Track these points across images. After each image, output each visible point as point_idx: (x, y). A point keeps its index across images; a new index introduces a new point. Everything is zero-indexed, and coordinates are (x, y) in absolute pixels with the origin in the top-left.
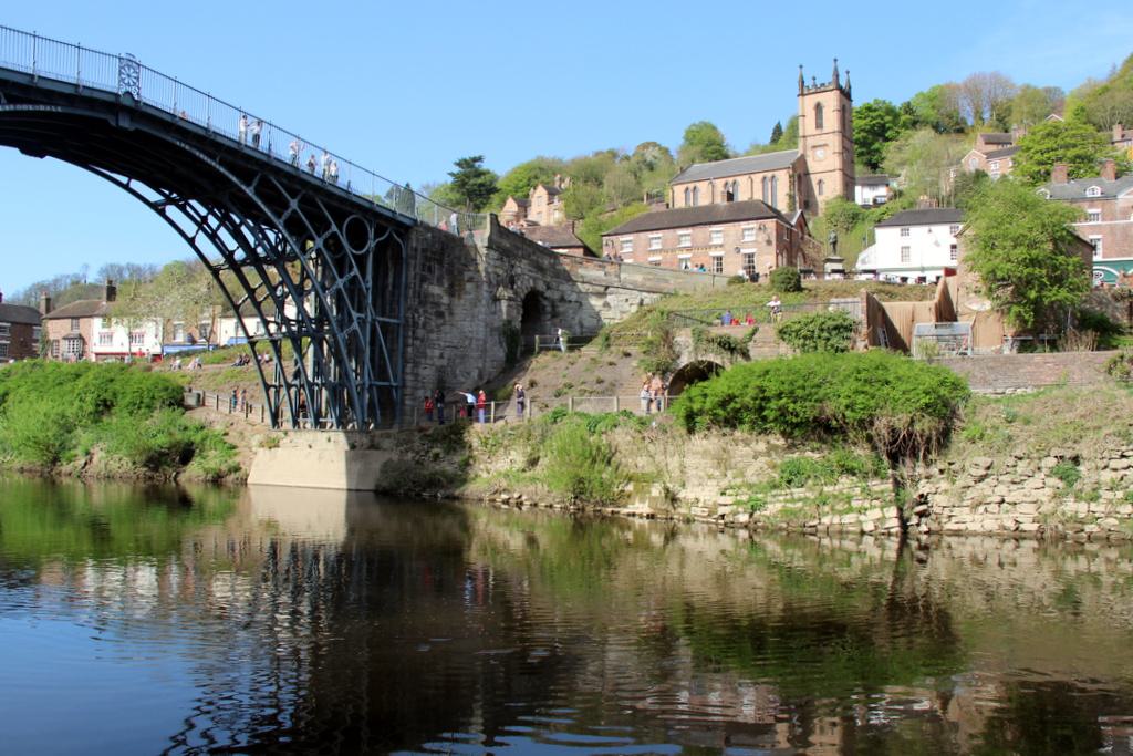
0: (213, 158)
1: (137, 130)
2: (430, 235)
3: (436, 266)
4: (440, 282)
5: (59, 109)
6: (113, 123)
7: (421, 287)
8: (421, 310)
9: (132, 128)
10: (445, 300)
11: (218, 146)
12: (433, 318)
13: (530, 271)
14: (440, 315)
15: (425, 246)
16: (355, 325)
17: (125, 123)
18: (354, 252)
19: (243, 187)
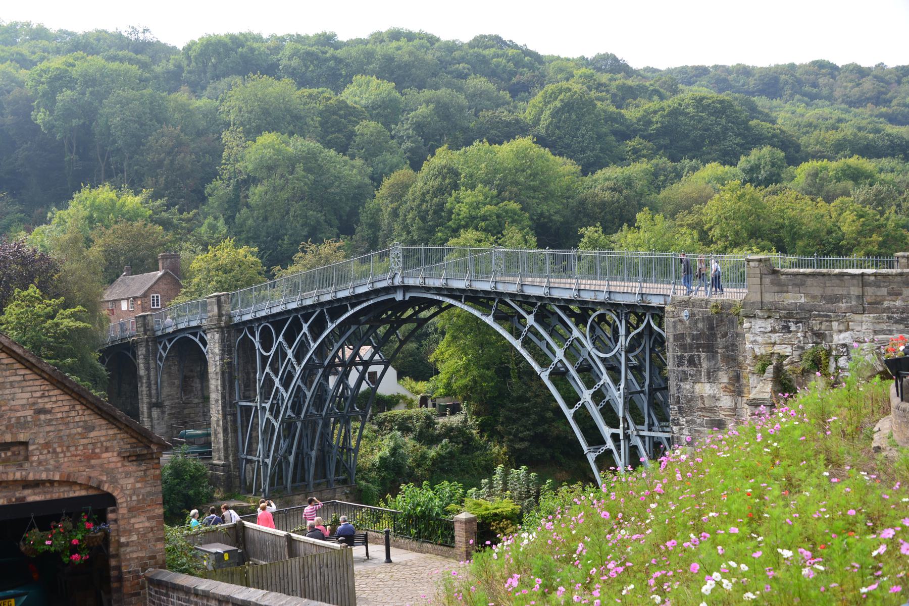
0: (460, 301)
1: (410, 297)
2: (685, 313)
3: (703, 355)
4: (711, 377)
5: (372, 302)
6: (397, 300)
7: (679, 388)
8: (683, 421)
9: (407, 298)
10: (726, 401)
11: (452, 290)
12: (707, 430)
13: (876, 332)
14: (720, 425)
15: (680, 329)
16: (610, 444)
17: (399, 297)
18: (602, 355)
19: (484, 318)
